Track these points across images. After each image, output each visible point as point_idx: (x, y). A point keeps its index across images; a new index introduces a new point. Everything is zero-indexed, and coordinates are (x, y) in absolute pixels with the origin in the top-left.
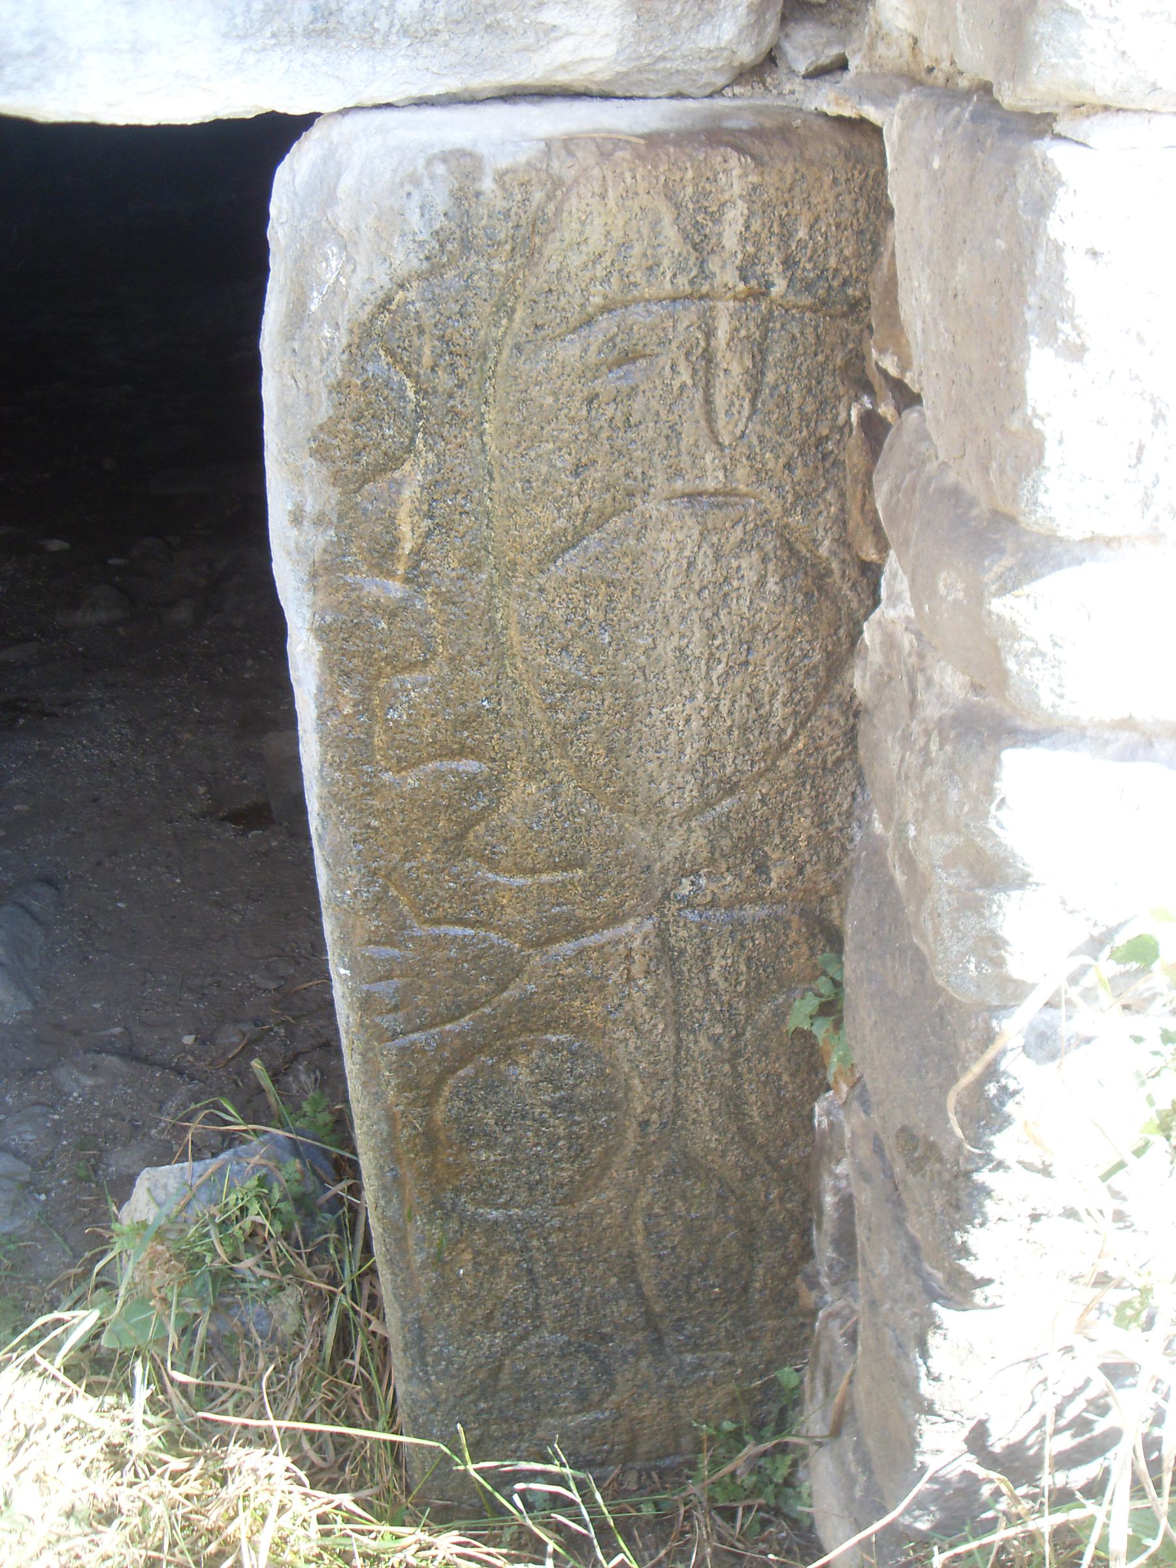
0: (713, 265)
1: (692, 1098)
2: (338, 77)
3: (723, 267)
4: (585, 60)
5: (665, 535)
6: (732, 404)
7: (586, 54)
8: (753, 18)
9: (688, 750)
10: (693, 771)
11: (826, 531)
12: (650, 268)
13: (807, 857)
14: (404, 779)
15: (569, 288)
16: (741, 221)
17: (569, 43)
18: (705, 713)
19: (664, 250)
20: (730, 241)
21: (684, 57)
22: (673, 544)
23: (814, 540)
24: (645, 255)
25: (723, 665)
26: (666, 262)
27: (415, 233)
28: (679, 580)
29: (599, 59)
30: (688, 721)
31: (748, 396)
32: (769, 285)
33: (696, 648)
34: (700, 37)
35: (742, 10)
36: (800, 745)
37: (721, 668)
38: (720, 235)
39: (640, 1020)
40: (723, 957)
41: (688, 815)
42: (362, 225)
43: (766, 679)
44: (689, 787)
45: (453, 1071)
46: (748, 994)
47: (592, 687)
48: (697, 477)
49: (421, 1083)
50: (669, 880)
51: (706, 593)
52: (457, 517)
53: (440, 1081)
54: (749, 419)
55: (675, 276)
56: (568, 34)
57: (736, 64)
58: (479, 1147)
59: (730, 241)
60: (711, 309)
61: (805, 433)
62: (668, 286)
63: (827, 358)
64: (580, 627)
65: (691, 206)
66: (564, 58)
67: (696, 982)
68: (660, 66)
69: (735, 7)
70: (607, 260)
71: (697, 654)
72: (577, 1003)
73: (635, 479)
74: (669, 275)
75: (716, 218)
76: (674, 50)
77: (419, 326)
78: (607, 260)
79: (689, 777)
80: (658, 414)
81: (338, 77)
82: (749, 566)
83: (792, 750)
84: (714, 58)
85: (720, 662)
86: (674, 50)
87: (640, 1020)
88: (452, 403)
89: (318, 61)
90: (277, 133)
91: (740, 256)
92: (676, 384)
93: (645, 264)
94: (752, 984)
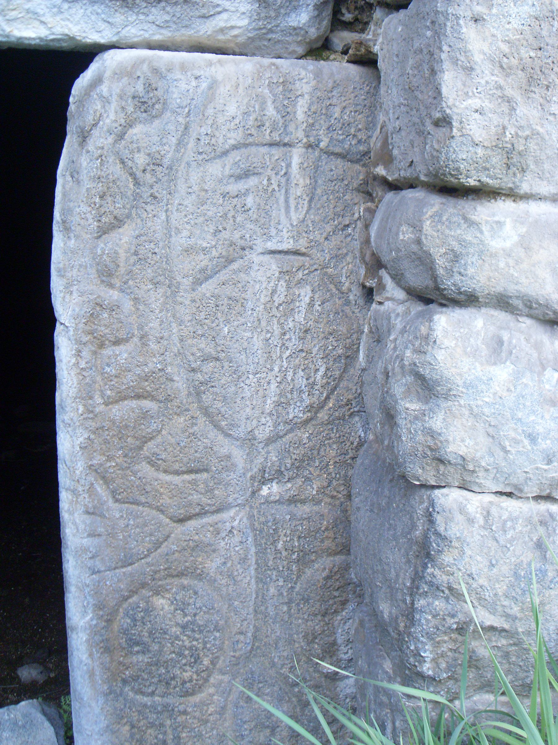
0: (291, 128)
1: (264, 628)
2: (109, 22)
3: (297, 128)
4: (232, 27)
5: (259, 273)
6: (298, 203)
7: (233, 23)
8: (316, 13)
9: (269, 402)
10: (271, 414)
11: (347, 278)
12: (259, 127)
13: (333, 475)
14: (111, 410)
15: (217, 134)
16: (306, 106)
17: (224, 16)
18: (278, 379)
19: (266, 118)
20: (300, 115)
21: (282, 31)
22: (265, 278)
23: (340, 282)
24: (256, 119)
25: (289, 351)
26: (267, 124)
27: (140, 98)
28: (268, 299)
29: (240, 28)
30: (269, 383)
31: (307, 199)
32: (319, 141)
33: (275, 340)
34: (290, 20)
35: (311, 8)
36: (331, 405)
37: (288, 353)
38: (295, 113)
39: (236, 573)
40: (285, 535)
41: (269, 441)
42: (114, 93)
43: (313, 361)
44: (268, 424)
45: (126, 599)
46: (298, 561)
47: (217, 359)
48: (279, 242)
49: (106, 614)
50: (256, 484)
51: (281, 308)
52: (150, 255)
53: (119, 604)
54: (307, 212)
55: (271, 132)
56: (226, 10)
57: (308, 40)
58: (138, 652)
59: (300, 115)
60: (290, 151)
61: (336, 222)
62: (268, 137)
63: (349, 182)
64: (213, 322)
65: (281, 96)
66: (222, 24)
67: (269, 550)
68: (270, 36)
69: (308, 5)
70: (237, 121)
71: (275, 343)
72: (200, 559)
73: (246, 240)
74: (268, 131)
75: (294, 102)
76: (277, 26)
77: (138, 147)
78: (237, 121)
79: (268, 418)
80: (259, 205)
81: (109, 22)
82: (305, 294)
83: (326, 408)
84: (297, 35)
85: (288, 349)
86: (277, 26)
87: (236, 573)
88: (152, 191)
89: (99, 11)
90: (80, 57)
91: (305, 124)
92: (270, 189)
93: (257, 124)
94: (301, 554)
